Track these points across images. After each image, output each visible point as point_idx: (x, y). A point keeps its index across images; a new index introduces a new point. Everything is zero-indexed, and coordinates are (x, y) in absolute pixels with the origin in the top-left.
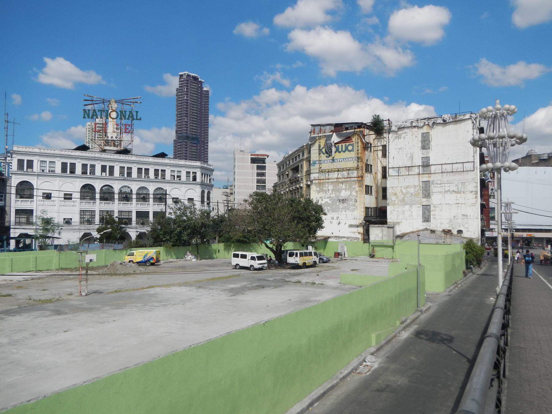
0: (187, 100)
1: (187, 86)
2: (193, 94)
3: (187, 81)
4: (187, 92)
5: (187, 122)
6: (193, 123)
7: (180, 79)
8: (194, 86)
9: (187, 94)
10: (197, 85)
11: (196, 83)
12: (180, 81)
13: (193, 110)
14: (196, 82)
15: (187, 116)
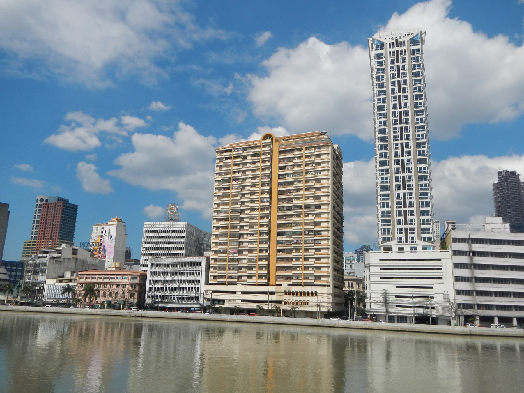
0: (508, 193)
1: (507, 181)
2: (513, 187)
3: (506, 176)
4: (507, 186)
5: (510, 213)
6: (517, 214)
7: (498, 176)
8: (513, 180)
9: (508, 189)
10: (515, 179)
11: (514, 178)
12: (499, 178)
13: (515, 201)
14: (515, 176)
15: (510, 208)
